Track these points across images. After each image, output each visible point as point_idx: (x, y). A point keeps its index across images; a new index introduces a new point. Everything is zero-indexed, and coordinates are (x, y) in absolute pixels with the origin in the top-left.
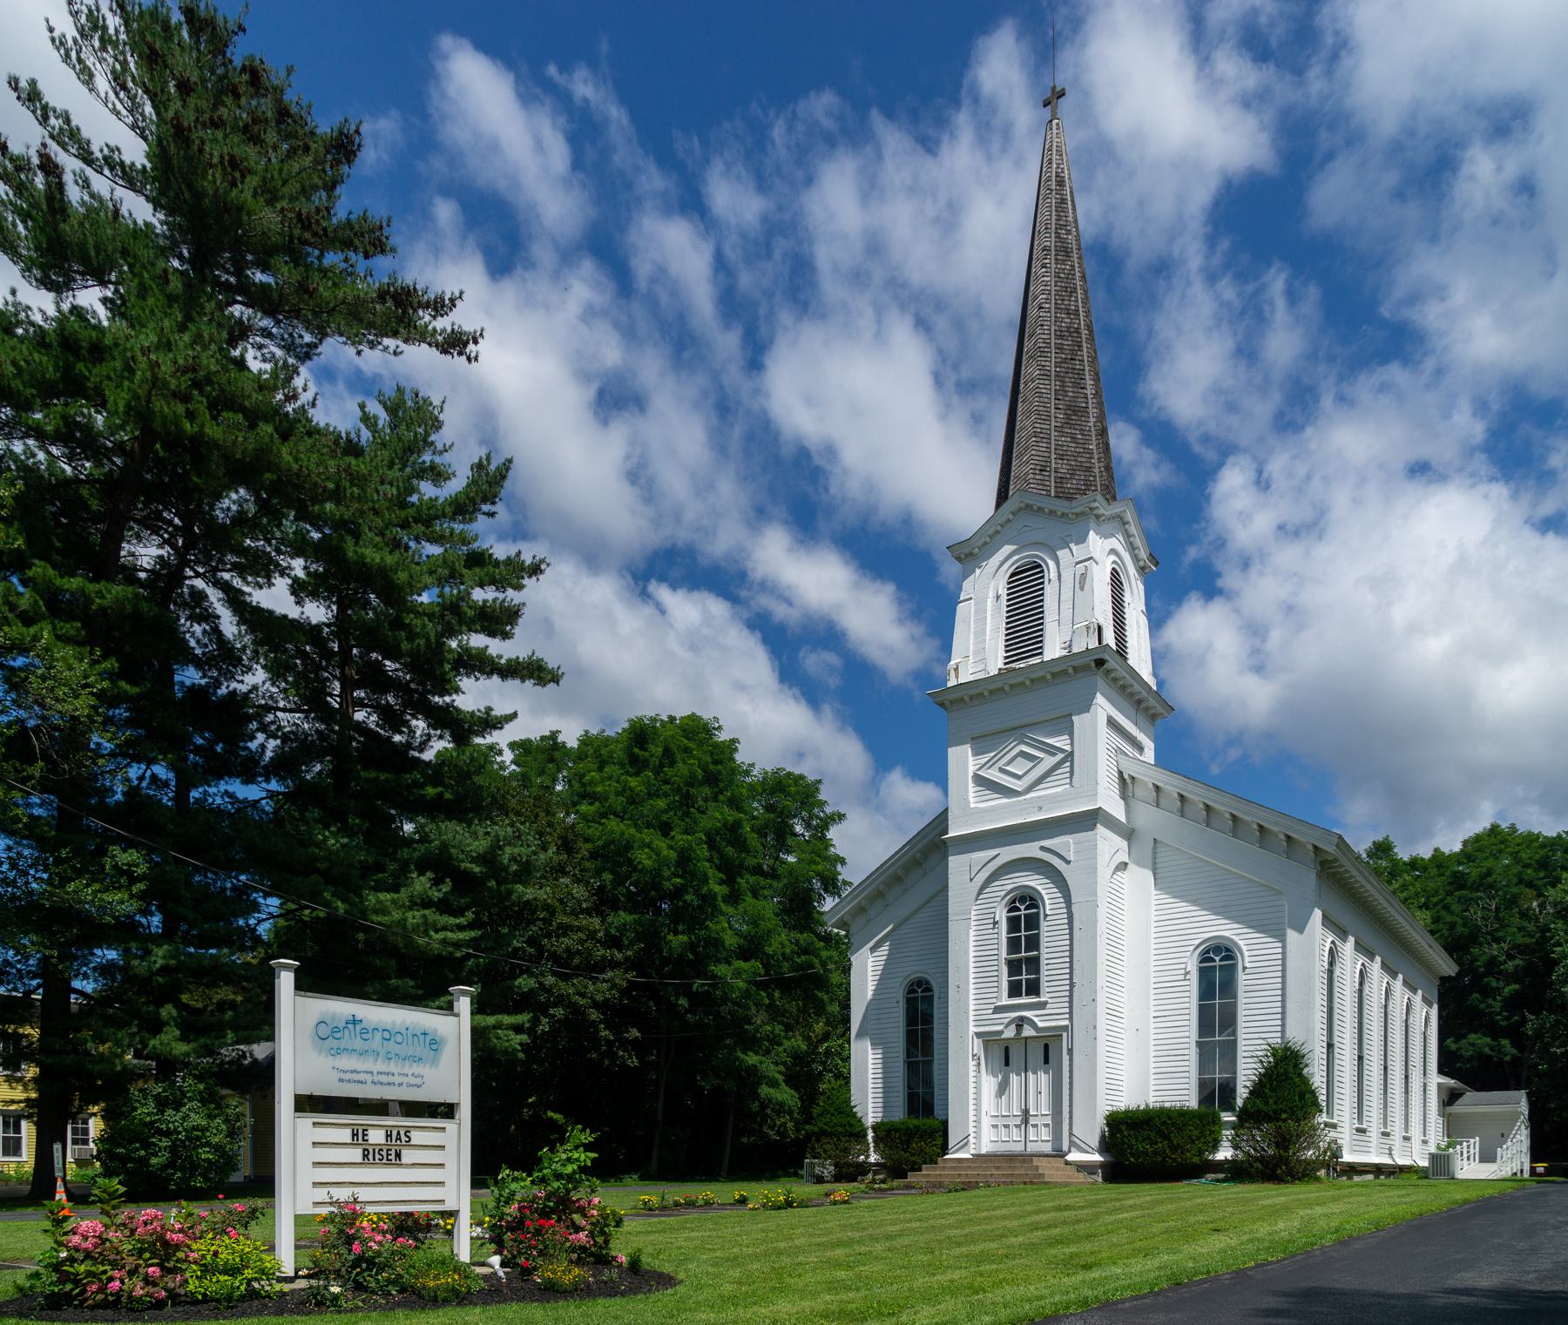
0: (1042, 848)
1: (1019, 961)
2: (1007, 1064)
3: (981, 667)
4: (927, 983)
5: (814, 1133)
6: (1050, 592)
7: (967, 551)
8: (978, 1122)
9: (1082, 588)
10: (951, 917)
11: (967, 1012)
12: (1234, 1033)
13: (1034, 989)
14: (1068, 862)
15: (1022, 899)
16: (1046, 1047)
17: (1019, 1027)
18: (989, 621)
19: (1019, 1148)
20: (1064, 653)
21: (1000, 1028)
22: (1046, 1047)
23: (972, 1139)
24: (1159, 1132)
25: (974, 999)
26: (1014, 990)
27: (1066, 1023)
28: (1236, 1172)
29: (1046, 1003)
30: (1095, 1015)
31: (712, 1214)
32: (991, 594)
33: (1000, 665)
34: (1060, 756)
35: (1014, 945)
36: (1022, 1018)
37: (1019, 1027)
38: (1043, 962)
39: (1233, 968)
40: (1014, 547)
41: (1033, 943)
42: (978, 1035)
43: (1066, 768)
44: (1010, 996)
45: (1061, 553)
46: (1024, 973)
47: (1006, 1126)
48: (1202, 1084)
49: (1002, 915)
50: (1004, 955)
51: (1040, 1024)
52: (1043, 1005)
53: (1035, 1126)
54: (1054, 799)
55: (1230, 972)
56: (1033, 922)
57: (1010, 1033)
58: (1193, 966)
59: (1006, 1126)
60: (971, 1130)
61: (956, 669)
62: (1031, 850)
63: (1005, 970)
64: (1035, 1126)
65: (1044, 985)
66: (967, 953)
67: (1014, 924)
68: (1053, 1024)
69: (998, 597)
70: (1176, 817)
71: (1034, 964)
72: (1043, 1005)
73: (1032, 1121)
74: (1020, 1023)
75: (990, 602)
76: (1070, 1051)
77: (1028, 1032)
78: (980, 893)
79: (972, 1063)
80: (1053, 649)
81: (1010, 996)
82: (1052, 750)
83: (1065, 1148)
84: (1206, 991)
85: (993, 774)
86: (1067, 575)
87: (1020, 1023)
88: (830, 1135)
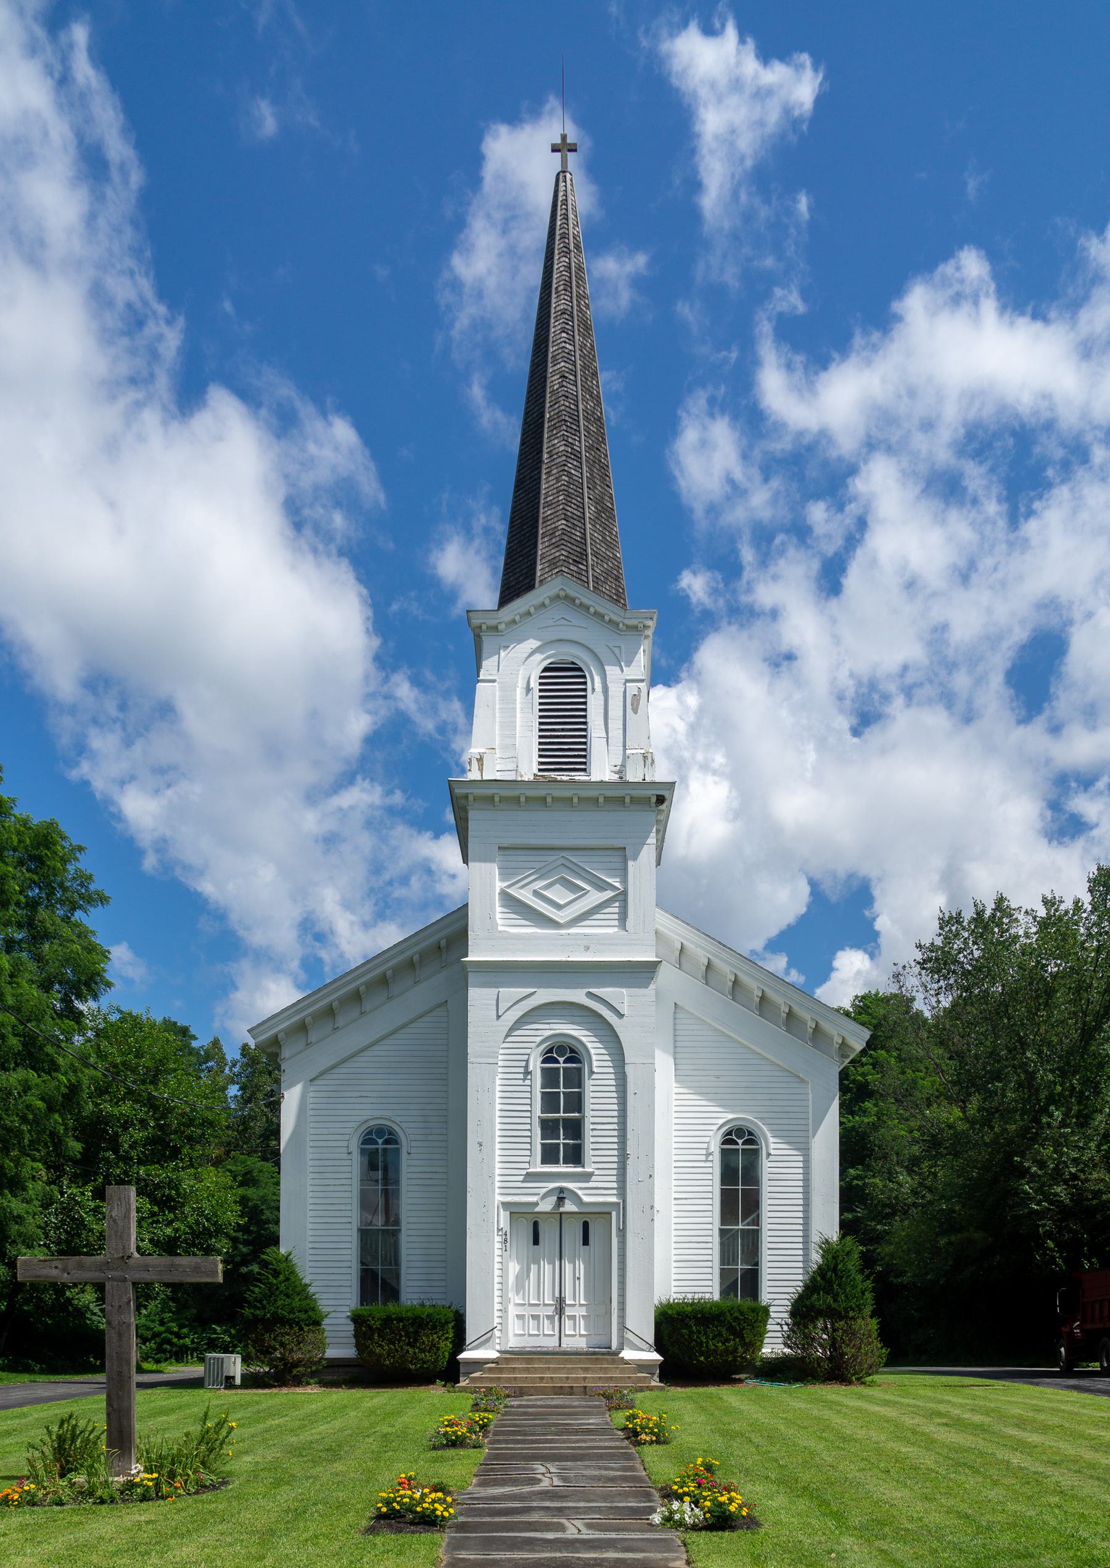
0: (590, 995)
1: (556, 1121)
2: (536, 1242)
3: (512, 766)
4: (391, 1132)
5: (262, 1320)
6: (594, 702)
7: (492, 622)
8: (504, 1311)
9: (635, 711)
10: (471, 1058)
11: (491, 1177)
12: (757, 1221)
13: (575, 1156)
14: (621, 1016)
15: (561, 1049)
16: (586, 1225)
17: (561, 1200)
18: (518, 715)
19: (551, 1343)
20: (615, 777)
21: (534, 1199)
22: (586, 1225)
23: (497, 1333)
24: (732, 1330)
25: (501, 1160)
26: (549, 1155)
27: (614, 1199)
28: (777, 1371)
29: (591, 1174)
30: (652, 1193)
31: (462, 1452)
32: (521, 684)
33: (535, 768)
34: (609, 894)
35: (550, 1102)
36: (562, 1190)
37: (561, 1200)
38: (588, 1126)
39: (756, 1153)
40: (538, 643)
41: (576, 1102)
42: (505, 1205)
43: (615, 909)
44: (544, 1161)
45: (612, 671)
46: (563, 1134)
47: (535, 1317)
48: (723, 1273)
49: (536, 1064)
50: (538, 1112)
51: (586, 1199)
52: (587, 1177)
53: (570, 1317)
54: (601, 941)
55: (753, 1156)
56: (575, 1079)
57: (547, 1206)
58: (715, 1147)
59: (535, 1317)
60: (497, 1320)
61: (480, 760)
62: (578, 996)
63: (538, 1131)
64: (570, 1317)
65: (588, 1153)
66: (492, 1104)
67: (550, 1078)
68: (601, 1199)
69: (528, 689)
70: (700, 984)
71: (575, 1129)
72: (587, 1177)
73: (568, 1312)
74: (561, 1196)
75: (519, 692)
76: (622, 1232)
77: (569, 1207)
78: (507, 1036)
79: (498, 1239)
80: (602, 769)
81: (544, 1161)
82: (601, 886)
83: (614, 1345)
84: (728, 1174)
85: (525, 895)
86: (615, 690)
87: (561, 1196)
88: (290, 1323)
